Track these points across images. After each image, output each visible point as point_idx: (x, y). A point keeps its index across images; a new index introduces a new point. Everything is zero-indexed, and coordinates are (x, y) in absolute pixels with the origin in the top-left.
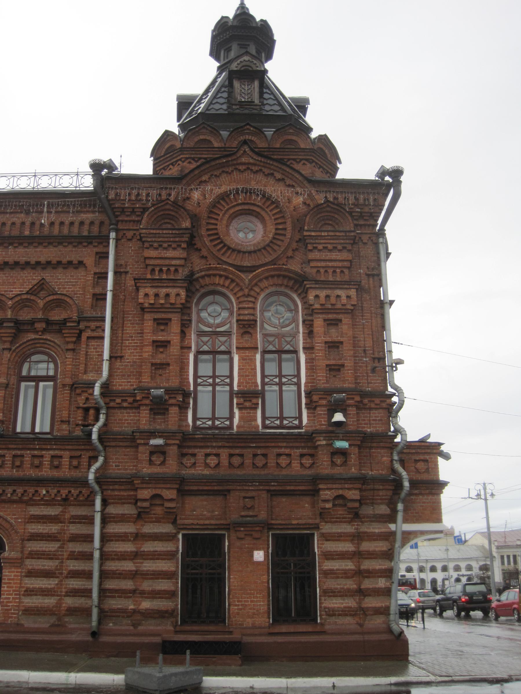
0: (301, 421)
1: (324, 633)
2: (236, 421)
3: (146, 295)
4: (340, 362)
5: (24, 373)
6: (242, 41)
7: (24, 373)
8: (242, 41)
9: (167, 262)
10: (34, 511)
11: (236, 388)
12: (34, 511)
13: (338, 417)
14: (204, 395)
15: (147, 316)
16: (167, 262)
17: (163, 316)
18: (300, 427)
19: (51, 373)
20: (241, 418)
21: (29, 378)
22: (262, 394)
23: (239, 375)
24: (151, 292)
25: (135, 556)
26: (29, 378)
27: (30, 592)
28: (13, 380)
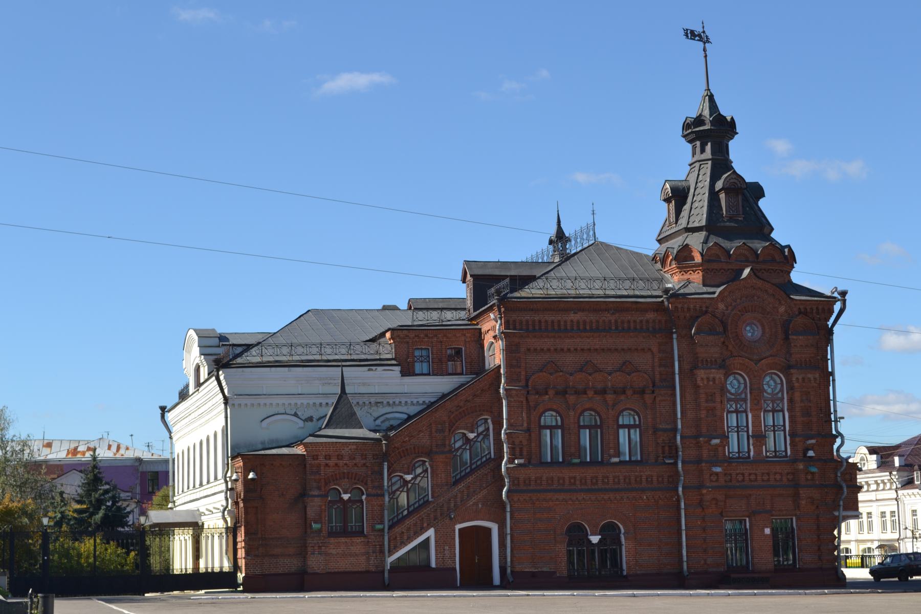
2: (752, 454)
3: (702, 379)
5: (621, 423)
7: (621, 423)
13: (811, 453)
14: (733, 438)
18: (786, 456)
20: (755, 452)
21: (624, 426)
22: (765, 437)
23: (753, 426)
26: (624, 426)
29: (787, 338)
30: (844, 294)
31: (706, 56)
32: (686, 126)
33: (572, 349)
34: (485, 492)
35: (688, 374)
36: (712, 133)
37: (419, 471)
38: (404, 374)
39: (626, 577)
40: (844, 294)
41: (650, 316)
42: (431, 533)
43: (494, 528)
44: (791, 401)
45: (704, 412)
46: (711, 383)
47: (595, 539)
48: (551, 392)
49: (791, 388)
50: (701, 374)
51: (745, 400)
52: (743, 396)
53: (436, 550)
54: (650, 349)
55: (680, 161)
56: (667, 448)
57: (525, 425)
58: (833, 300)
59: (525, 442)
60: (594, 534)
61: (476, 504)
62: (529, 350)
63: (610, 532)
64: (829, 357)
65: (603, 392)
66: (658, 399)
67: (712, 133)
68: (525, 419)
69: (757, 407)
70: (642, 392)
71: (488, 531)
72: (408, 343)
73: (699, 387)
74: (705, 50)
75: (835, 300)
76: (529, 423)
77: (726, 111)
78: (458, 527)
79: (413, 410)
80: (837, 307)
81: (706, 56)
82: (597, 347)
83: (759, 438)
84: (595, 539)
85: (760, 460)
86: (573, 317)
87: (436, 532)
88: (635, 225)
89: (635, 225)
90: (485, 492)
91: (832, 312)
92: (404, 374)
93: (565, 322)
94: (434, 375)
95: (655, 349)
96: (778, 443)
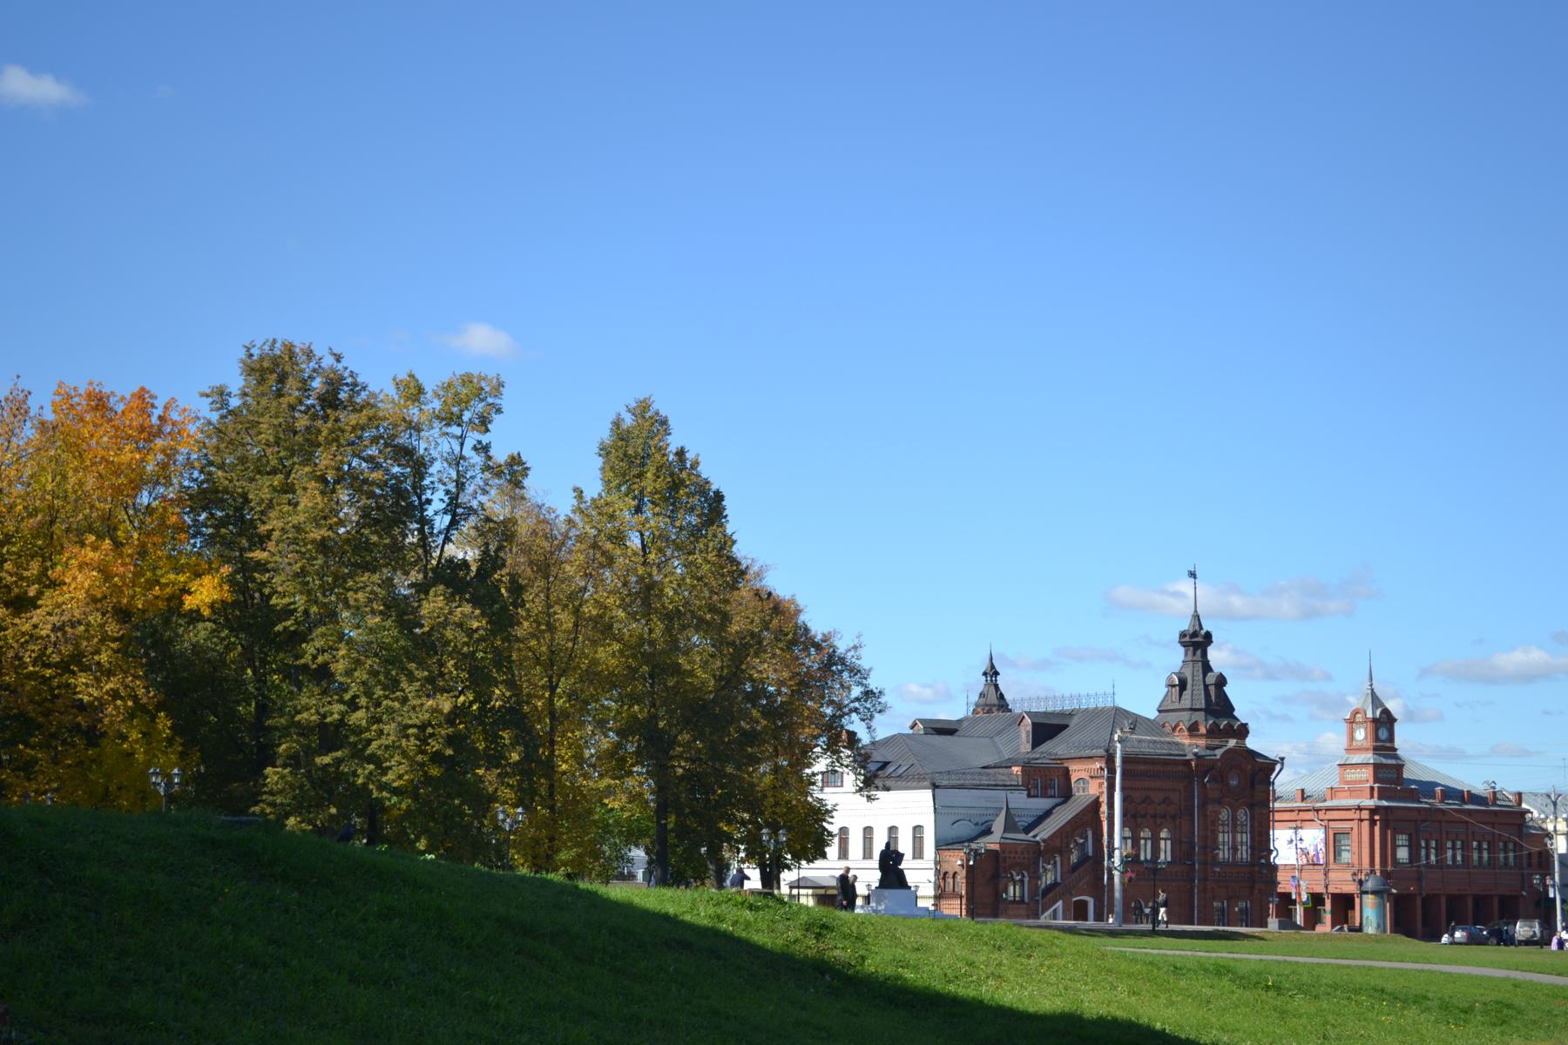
29: (1252, 786)
32: (1183, 635)
35: (1203, 805)
36: (1197, 642)
38: (1029, 796)
41: (1181, 768)
42: (1060, 903)
43: (1091, 901)
49: (1252, 818)
50: (1210, 808)
55: (1175, 658)
58: (1275, 762)
65: (1154, 816)
67: (1197, 642)
69: (1234, 831)
70: (1173, 817)
71: (1086, 903)
77: (1206, 627)
80: (1278, 768)
83: (1235, 849)
85: (1235, 864)
86: (1142, 767)
88: (1144, 696)
89: (1144, 696)
92: (1029, 796)
96: (1244, 854)
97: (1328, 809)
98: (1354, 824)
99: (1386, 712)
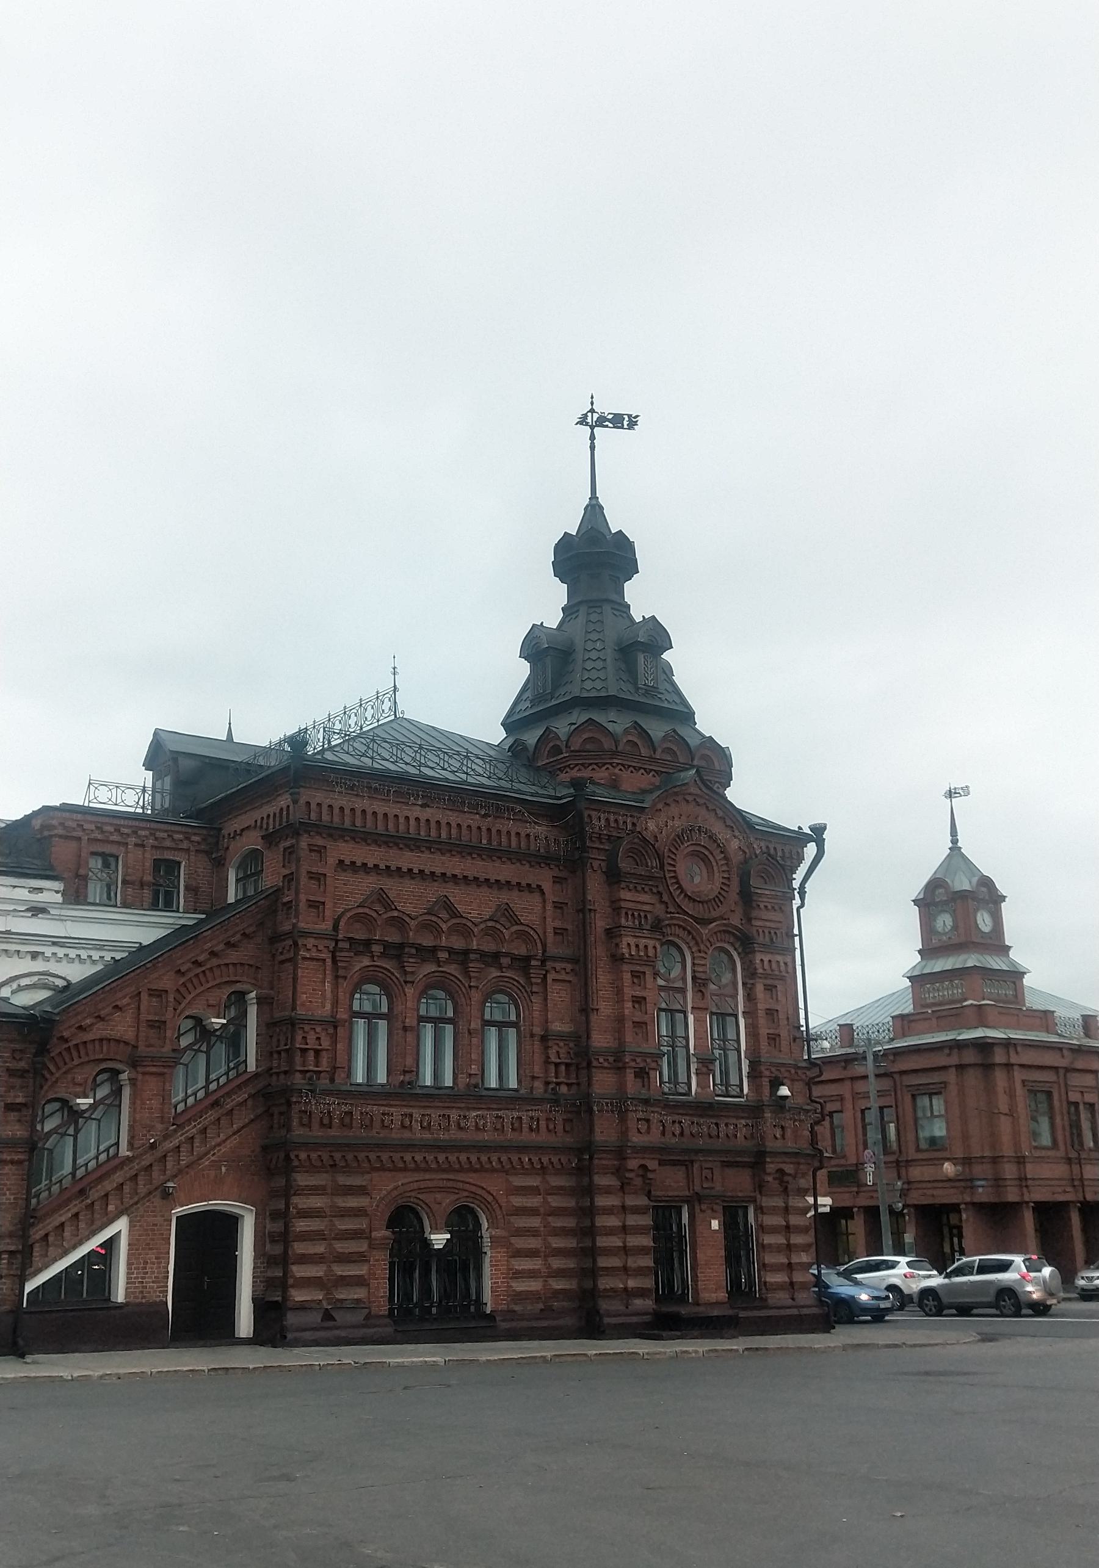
0: (742, 1090)
1: (767, 1307)
4: (777, 1032)
6: (594, 559)
8: (594, 559)
9: (639, 907)
10: (518, 1181)
11: (692, 1051)
12: (518, 1181)
15: (625, 967)
16: (639, 907)
17: (638, 968)
19: (513, 1018)
24: (632, 941)
25: (624, 1229)
27: (518, 1275)
28: (475, 1024)
30: (818, 831)
31: (592, 448)
33: (416, 871)
34: (234, 1141)
37: (101, 1093)
39: (491, 1317)
40: (818, 831)
42: (121, 1226)
44: (750, 997)
45: (629, 1005)
46: (642, 954)
47: (439, 1239)
48: (377, 949)
51: (683, 991)
52: (679, 984)
53: (129, 1264)
54: (539, 886)
56: (563, 1068)
57: (328, 1006)
58: (808, 839)
59: (326, 1043)
60: (436, 1229)
61: (216, 1165)
62: (341, 862)
63: (463, 1223)
64: (796, 931)
66: (550, 977)
68: (329, 994)
70: (523, 963)
71: (232, 1222)
72: (79, 839)
73: (622, 959)
74: (592, 437)
75: (808, 839)
76: (336, 1003)
78: (179, 1210)
79: (76, 973)
80: (811, 850)
81: (592, 448)
82: (457, 872)
84: (439, 1239)
87: (132, 1226)
90: (234, 1141)
91: (800, 859)
93: (407, 818)
94: (125, 905)
95: (547, 886)
97: (897, 1053)
98: (951, 1076)
99: (987, 883)
